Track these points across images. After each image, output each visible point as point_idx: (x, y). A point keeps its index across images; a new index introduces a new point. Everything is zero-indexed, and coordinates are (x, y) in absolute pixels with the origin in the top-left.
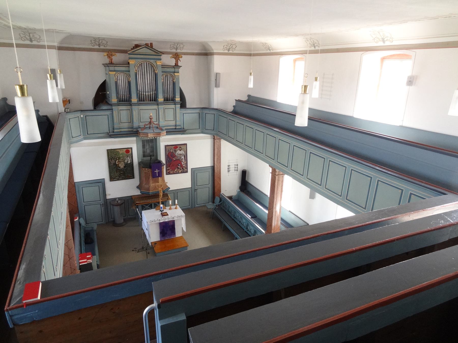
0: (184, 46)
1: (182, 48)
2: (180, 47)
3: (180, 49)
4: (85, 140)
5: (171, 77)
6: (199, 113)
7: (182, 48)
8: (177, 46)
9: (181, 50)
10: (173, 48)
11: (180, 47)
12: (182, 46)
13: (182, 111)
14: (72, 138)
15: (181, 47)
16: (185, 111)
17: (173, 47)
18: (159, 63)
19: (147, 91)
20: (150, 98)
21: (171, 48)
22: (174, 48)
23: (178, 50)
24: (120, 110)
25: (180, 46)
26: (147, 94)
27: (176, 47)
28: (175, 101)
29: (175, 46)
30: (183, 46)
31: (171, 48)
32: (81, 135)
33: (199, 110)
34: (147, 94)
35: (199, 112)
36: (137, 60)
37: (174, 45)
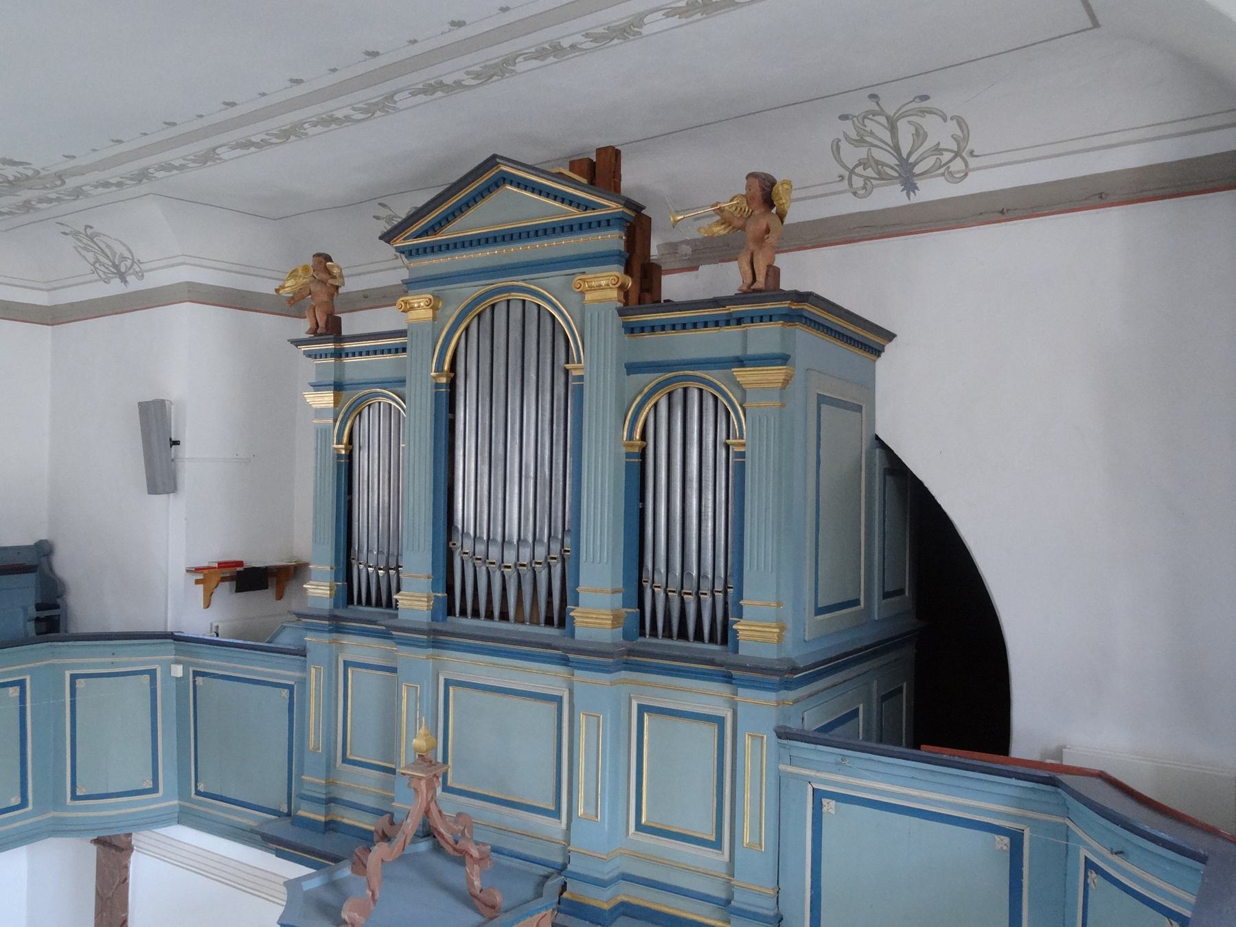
0: (961, 122)
1: (957, 154)
2: (928, 145)
3: (942, 170)
4: (179, 822)
5: (709, 403)
6: (1016, 839)
7: (957, 154)
8: (897, 149)
9: (951, 177)
10: (870, 172)
11: (928, 145)
12: (940, 133)
13: (806, 763)
14: (75, 797)
15: (937, 150)
16: (839, 767)
17: (863, 163)
18: (600, 288)
19: (499, 538)
20: (379, 589)
21: (858, 182)
22: (882, 177)
23: (919, 183)
24: (347, 664)
25: (920, 135)
26: (510, 557)
27: (893, 161)
28: (736, 651)
29: (878, 154)
30: (953, 127)
31: (858, 182)
32: (155, 789)
33: (1019, 802)
34: (510, 557)
35: (1016, 818)
36: (452, 290)
37: (860, 142)
